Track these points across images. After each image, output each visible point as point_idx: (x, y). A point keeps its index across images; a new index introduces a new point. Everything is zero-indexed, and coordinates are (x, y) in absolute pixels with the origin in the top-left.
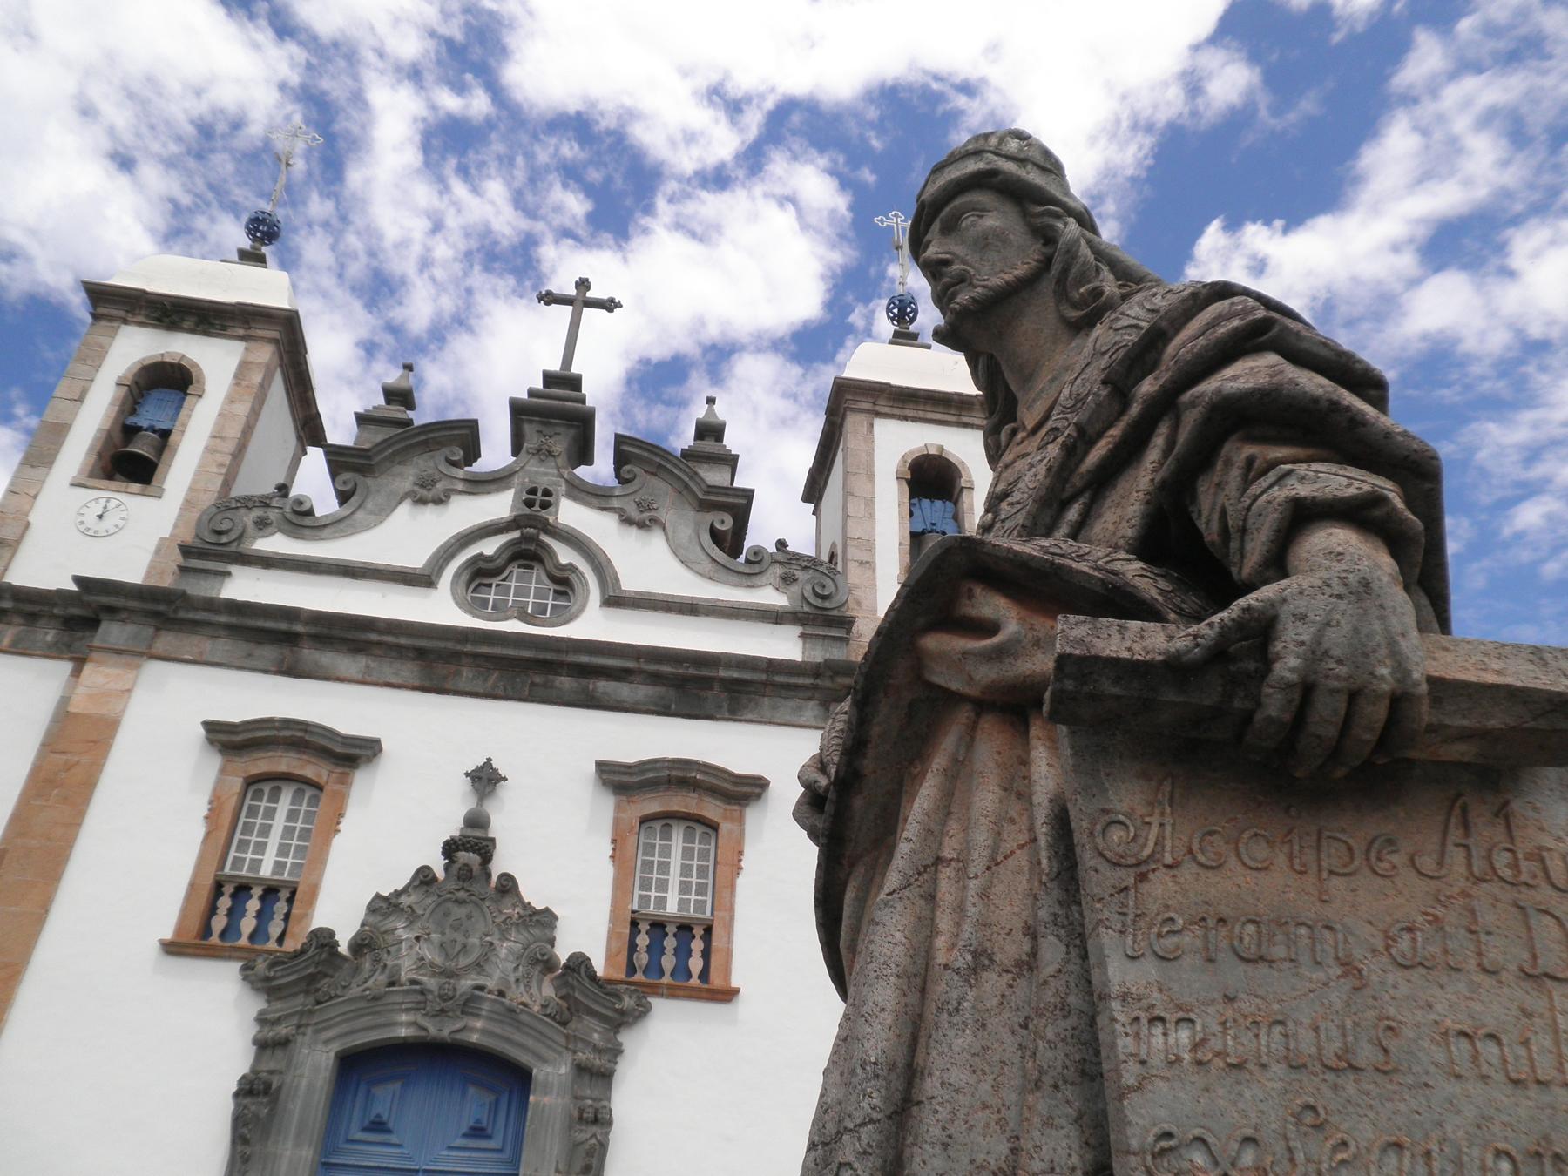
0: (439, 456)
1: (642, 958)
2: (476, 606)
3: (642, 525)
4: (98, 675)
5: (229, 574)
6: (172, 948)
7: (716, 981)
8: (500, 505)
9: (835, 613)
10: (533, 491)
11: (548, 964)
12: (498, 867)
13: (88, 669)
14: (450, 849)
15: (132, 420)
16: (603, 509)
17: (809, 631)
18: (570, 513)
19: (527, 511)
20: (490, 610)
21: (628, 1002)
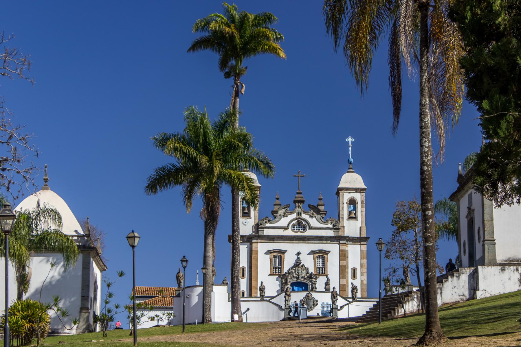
0: (286, 209)
1: (318, 272)
2: (294, 230)
3: (312, 217)
4: (254, 245)
5: (264, 230)
6: (270, 275)
7: (326, 274)
8: (294, 216)
9: (338, 227)
10: (298, 213)
11: (308, 273)
12: (302, 264)
13: (253, 244)
14: (297, 262)
15: (243, 206)
16: (308, 215)
17: (335, 230)
18: (304, 216)
19: (298, 217)
20: (296, 230)
21: (317, 276)
